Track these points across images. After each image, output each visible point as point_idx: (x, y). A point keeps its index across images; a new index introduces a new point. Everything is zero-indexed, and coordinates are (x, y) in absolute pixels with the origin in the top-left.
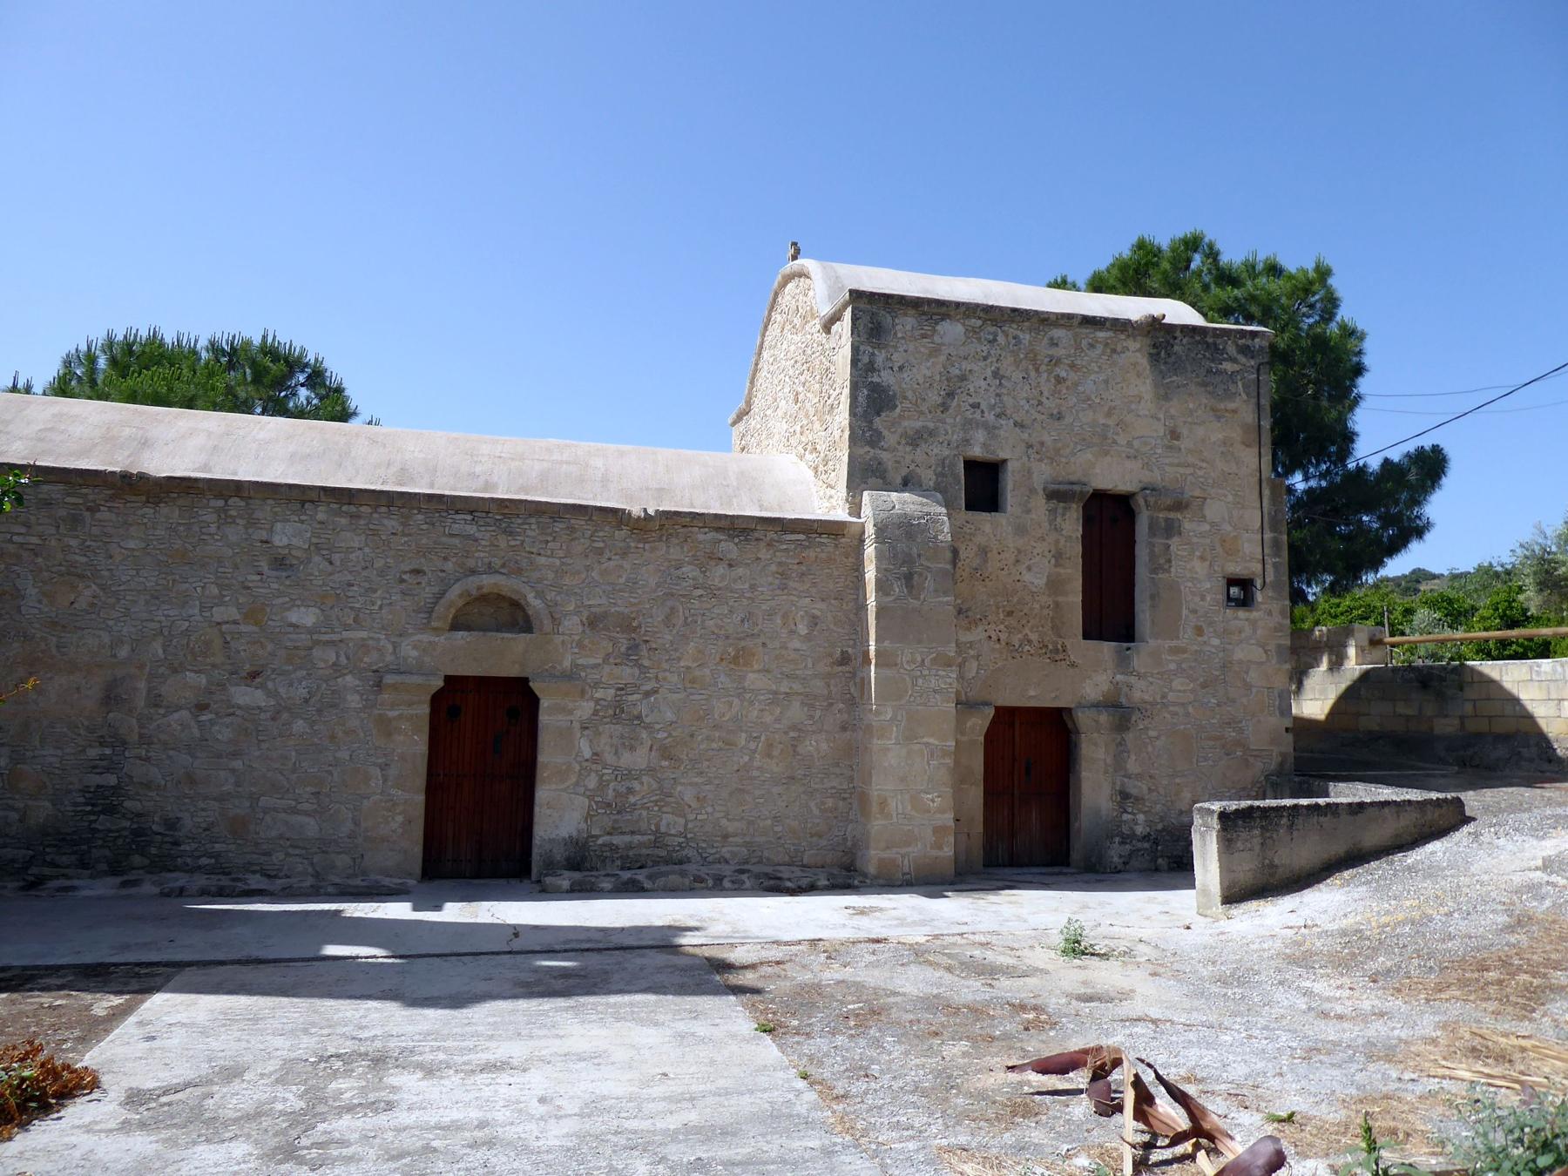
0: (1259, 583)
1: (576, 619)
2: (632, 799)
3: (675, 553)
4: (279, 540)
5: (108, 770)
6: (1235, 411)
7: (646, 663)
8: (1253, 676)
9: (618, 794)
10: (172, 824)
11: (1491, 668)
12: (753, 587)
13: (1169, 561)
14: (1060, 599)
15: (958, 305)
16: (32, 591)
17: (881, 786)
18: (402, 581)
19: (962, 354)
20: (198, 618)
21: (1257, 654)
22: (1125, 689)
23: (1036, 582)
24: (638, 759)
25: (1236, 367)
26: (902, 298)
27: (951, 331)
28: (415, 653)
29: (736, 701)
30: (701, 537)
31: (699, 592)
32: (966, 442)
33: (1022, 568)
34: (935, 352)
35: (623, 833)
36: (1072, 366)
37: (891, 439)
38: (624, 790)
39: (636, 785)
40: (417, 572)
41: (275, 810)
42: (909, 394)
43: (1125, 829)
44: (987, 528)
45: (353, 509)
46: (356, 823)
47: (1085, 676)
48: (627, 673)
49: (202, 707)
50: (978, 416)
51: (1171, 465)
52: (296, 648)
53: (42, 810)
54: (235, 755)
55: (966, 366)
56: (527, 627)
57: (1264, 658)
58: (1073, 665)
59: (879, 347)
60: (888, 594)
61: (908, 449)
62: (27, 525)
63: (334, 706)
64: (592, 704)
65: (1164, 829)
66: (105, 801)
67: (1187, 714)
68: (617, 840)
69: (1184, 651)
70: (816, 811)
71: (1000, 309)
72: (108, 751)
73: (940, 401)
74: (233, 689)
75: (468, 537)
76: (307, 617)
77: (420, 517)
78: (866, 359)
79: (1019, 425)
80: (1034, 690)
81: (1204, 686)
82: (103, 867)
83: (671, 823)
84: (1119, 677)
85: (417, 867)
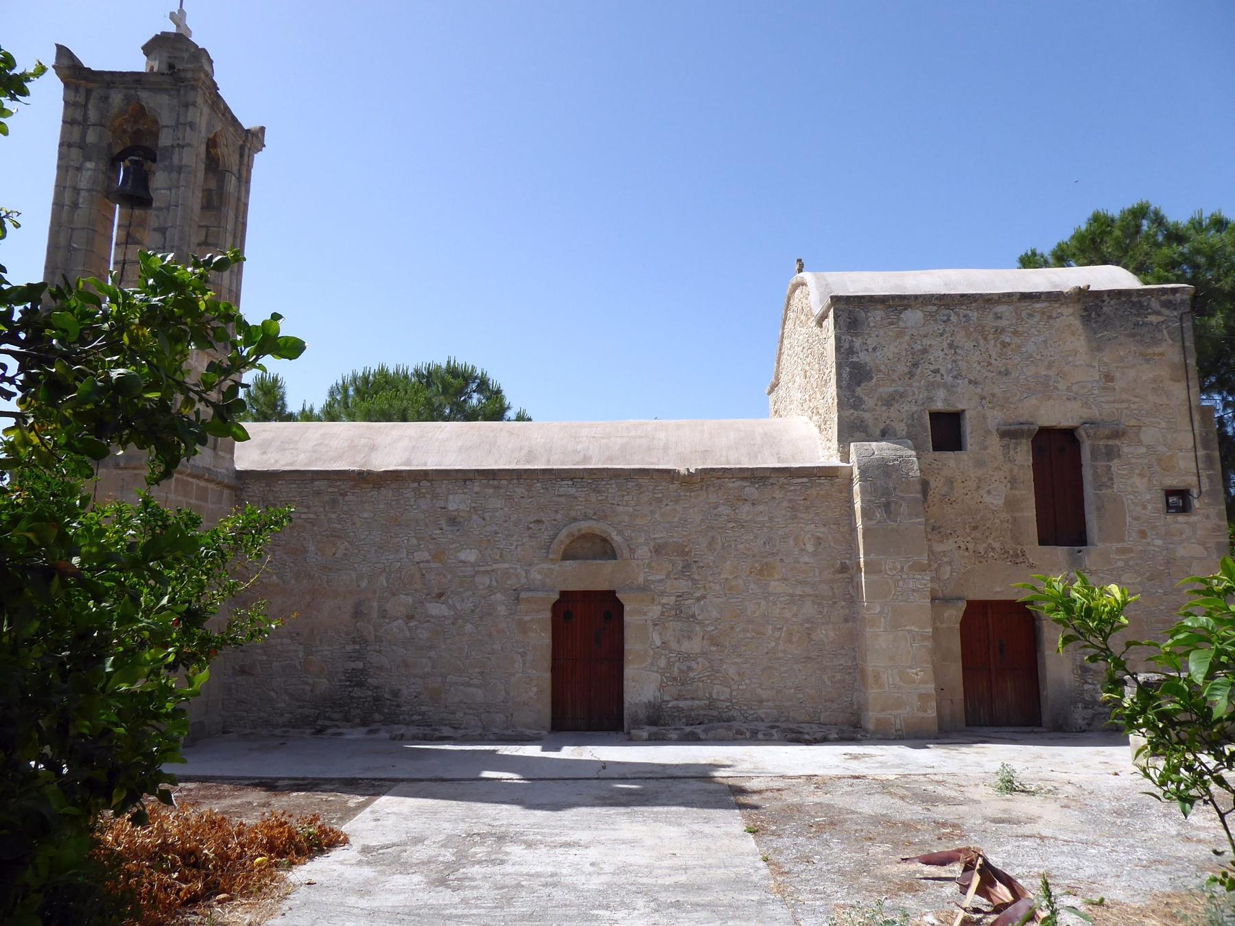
0: (1195, 492)
1: (646, 548)
2: (691, 675)
3: (713, 498)
4: (452, 507)
5: (358, 659)
6: (1162, 354)
7: (696, 577)
9: (681, 671)
10: (396, 693)
12: (771, 519)
13: (1112, 479)
14: (1017, 515)
15: (916, 297)
16: (312, 548)
17: (874, 663)
18: (529, 528)
21: (1198, 551)
24: (694, 645)
25: (1161, 319)
26: (872, 297)
27: (913, 317)
28: (539, 577)
29: (763, 603)
30: (731, 485)
32: (931, 399)
33: (983, 492)
34: (900, 334)
36: (1015, 333)
37: (869, 402)
38: (685, 668)
39: (694, 665)
40: (538, 522)
41: (456, 683)
42: (882, 368)
43: (1087, 697)
44: (952, 463)
45: (496, 482)
48: (683, 585)
49: (410, 617)
50: (938, 378)
51: (1107, 402)
53: (323, 684)
54: (431, 648)
55: (926, 342)
56: (613, 556)
57: (1205, 554)
58: (1032, 566)
59: (856, 335)
61: (884, 408)
62: (308, 507)
63: (490, 614)
64: (660, 608)
66: (356, 679)
68: (682, 704)
70: (829, 683)
72: (357, 647)
73: (907, 370)
76: (470, 556)
78: (847, 345)
79: (973, 382)
81: (1151, 579)
82: (357, 720)
83: (720, 692)
85: (547, 721)
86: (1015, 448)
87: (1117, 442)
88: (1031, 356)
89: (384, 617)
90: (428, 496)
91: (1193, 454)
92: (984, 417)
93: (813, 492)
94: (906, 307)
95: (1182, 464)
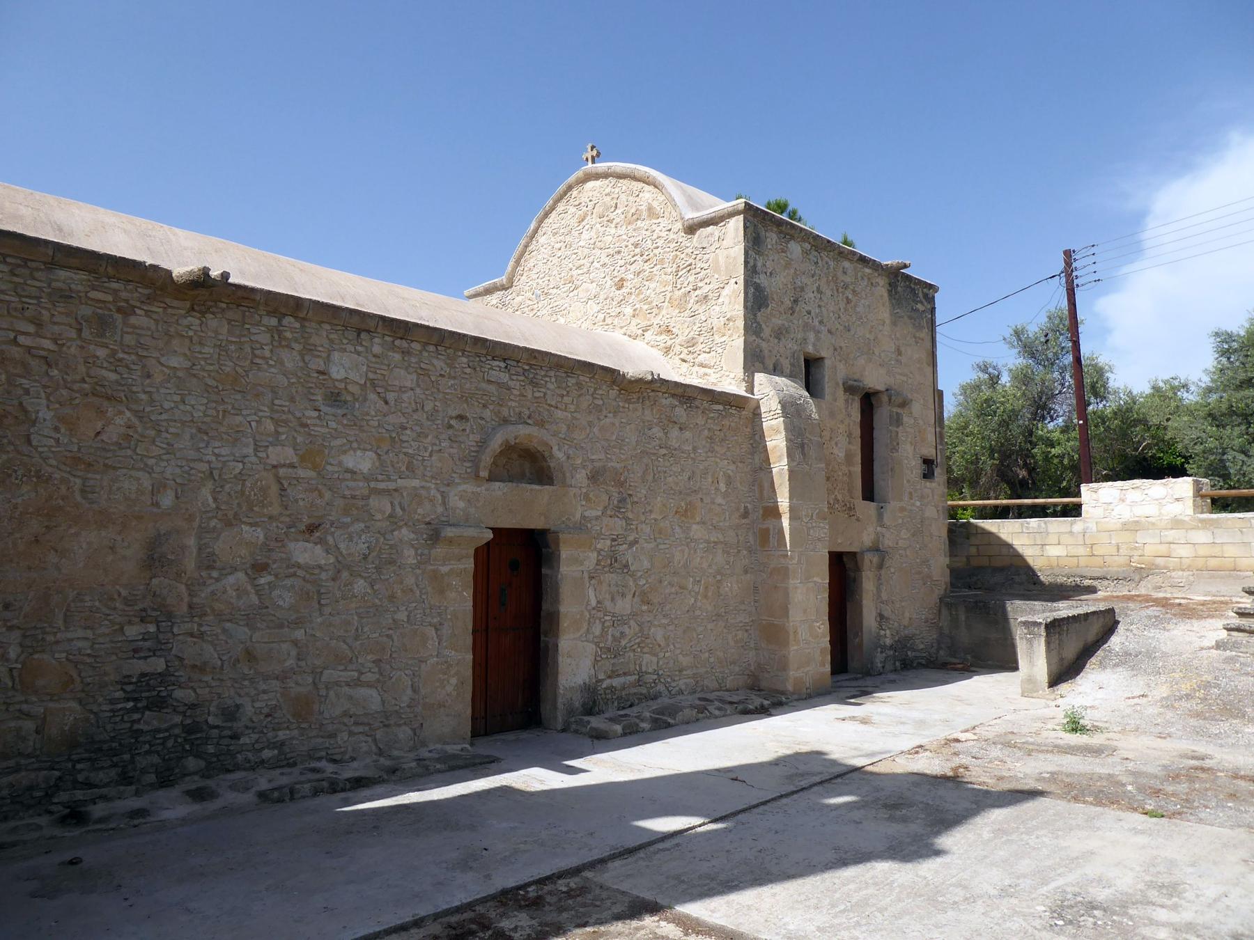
2: (623, 643)
3: (648, 415)
4: (337, 372)
7: (630, 515)
9: (615, 639)
11: (990, 525)
12: (695, 449)
16: (45, 414)
18: (450, 427)
20: (254, 459)
24: (624, 606)
27: (795, 248)
28: (462, 504)
30: (664, 401)
31: (664, 451)
35: (618, 676)
37: (767, 332)
38: (618, 634)
39: (626, 629)
40: (461, 417)
41: (337, 684)
45: (404, 344)
46: (415, 690)
48: (619, 524)
52: (353, 497)
58: (858, 520)
63: (392, 562)
64: (595, 554)
68: (616, 682)
70: (732, 643)
74: (292, 545)
75: (499, 385)
76: (363, 462)
77: (465, 360)
78: (752, 263)
83: (649, 662)
85: (467, 728)
89: (210, 568)
90: (297, 347)
93: (726, 422)
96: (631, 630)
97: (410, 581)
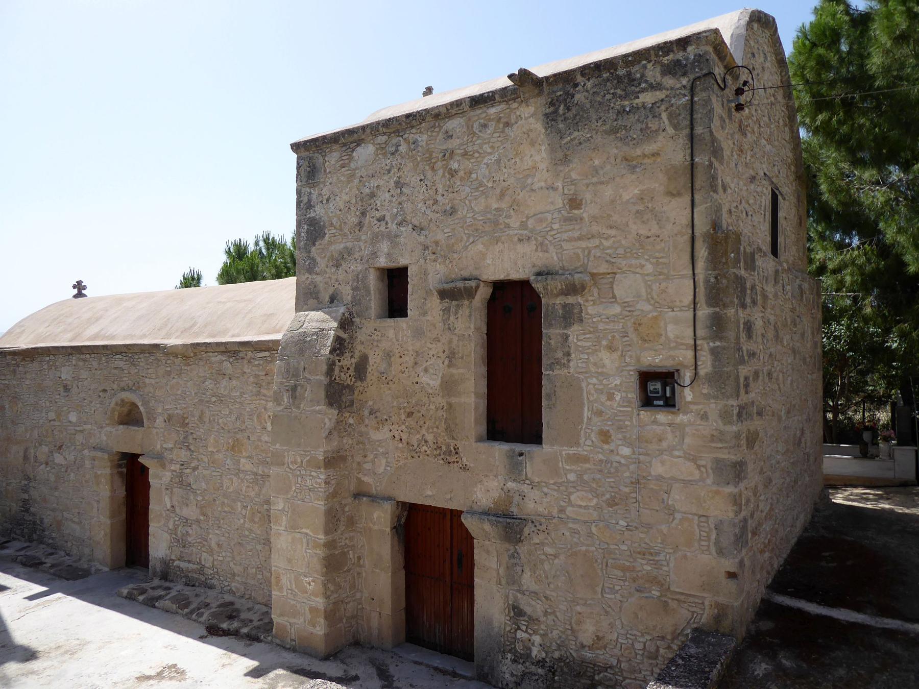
0: (687, 376)
6: (655, 154)
8: (677, 497)
12: (242, 393)
13: (568, 354)
14: (454, 400)
15: (363, 128)
16: (7, 406)
17: (278, 563)
19: (370, 172)
21: (687, 469)
22: (517, 498)
23: (431, 382)
24: (191, 512)
25: (660, 95)
26: (324, 137)
27: (365, 152)
29: (235, 479)
30: (213, 359)
31: (214, 399)
32: (374, 255)
33: (419, 370)
35: (185, 561)
36: (465, 154)
37: (322, 263)
43: (519, 647)
44: (391, 333)
47: (478, 480)
51: (570, 240)
57: (697, 475)
58: (464, 468)
59: (313, 186)
60: (279, 404)
61: (333, 269)
65: (560, 659)
67: (590, 535)
68: (183, 565)
69: (586, 460)
71: (396, 119)
73: (355, 220)
78: (305, 199)
80: (430, 494)
81: (612, 503)
83: (207, 559)
84: (510, 485)
86: (456, 313)
87: (580, 300)
88: (481, 185)
91: (690, 314)
92: (426, 274)
94: (359, 142)
95: (672, 331)
96: (193, 531)
97: (88, 476)
